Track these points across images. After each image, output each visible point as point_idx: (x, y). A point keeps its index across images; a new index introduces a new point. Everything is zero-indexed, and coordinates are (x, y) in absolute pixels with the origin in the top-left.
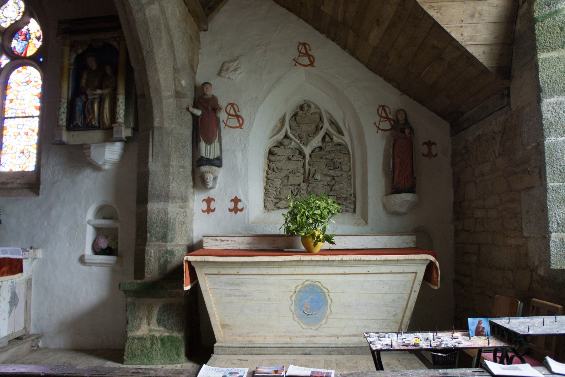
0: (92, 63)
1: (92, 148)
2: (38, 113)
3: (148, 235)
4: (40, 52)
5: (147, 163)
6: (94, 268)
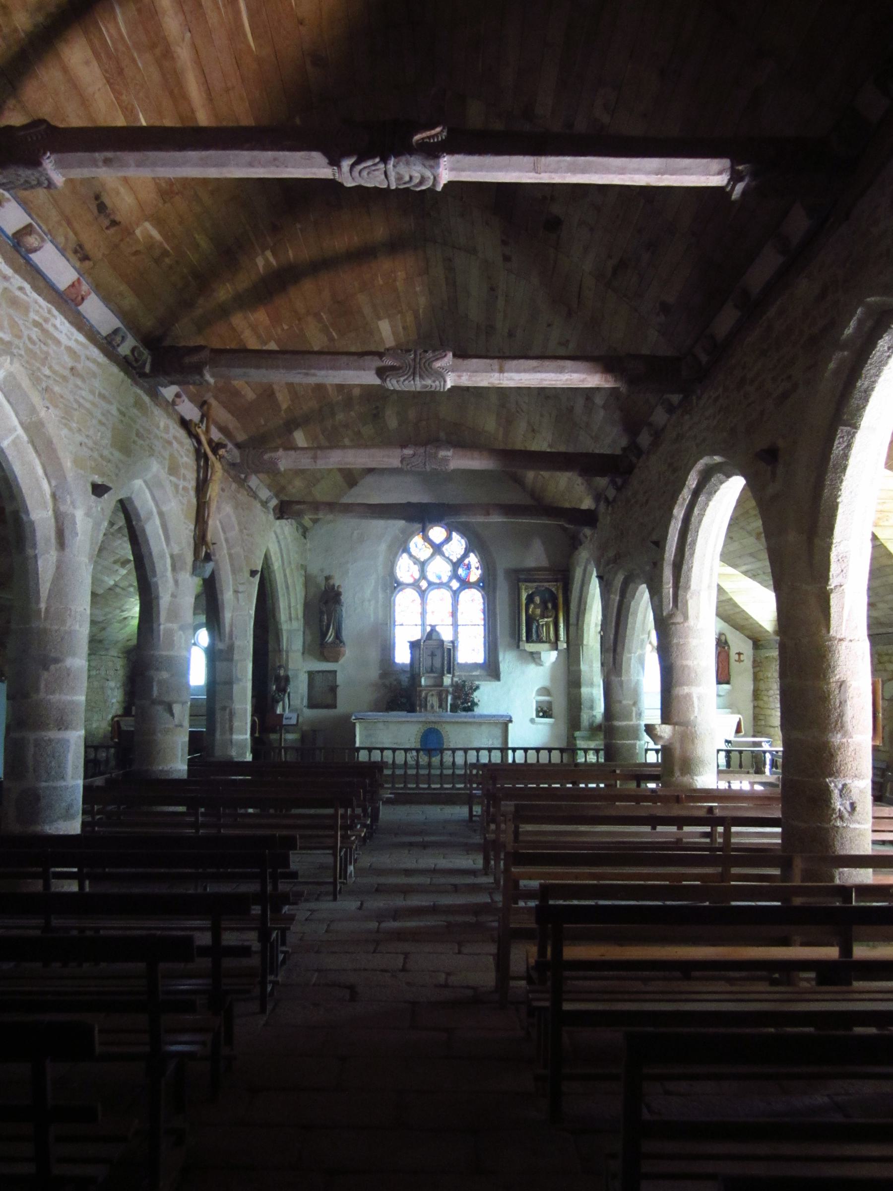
0: (537, 600)
1: (542, 654)
2: (482, 623)
3: (582, 706)
4: (481, 580)
5: (580, 665)
6: (540, 727)
